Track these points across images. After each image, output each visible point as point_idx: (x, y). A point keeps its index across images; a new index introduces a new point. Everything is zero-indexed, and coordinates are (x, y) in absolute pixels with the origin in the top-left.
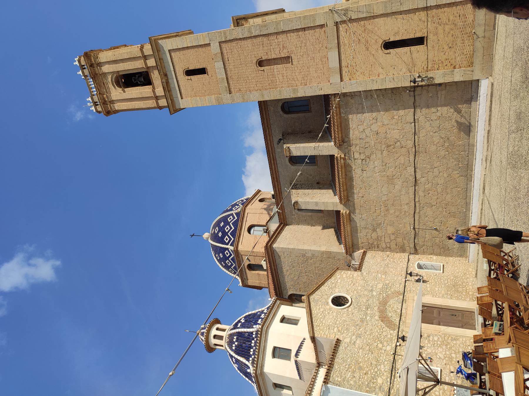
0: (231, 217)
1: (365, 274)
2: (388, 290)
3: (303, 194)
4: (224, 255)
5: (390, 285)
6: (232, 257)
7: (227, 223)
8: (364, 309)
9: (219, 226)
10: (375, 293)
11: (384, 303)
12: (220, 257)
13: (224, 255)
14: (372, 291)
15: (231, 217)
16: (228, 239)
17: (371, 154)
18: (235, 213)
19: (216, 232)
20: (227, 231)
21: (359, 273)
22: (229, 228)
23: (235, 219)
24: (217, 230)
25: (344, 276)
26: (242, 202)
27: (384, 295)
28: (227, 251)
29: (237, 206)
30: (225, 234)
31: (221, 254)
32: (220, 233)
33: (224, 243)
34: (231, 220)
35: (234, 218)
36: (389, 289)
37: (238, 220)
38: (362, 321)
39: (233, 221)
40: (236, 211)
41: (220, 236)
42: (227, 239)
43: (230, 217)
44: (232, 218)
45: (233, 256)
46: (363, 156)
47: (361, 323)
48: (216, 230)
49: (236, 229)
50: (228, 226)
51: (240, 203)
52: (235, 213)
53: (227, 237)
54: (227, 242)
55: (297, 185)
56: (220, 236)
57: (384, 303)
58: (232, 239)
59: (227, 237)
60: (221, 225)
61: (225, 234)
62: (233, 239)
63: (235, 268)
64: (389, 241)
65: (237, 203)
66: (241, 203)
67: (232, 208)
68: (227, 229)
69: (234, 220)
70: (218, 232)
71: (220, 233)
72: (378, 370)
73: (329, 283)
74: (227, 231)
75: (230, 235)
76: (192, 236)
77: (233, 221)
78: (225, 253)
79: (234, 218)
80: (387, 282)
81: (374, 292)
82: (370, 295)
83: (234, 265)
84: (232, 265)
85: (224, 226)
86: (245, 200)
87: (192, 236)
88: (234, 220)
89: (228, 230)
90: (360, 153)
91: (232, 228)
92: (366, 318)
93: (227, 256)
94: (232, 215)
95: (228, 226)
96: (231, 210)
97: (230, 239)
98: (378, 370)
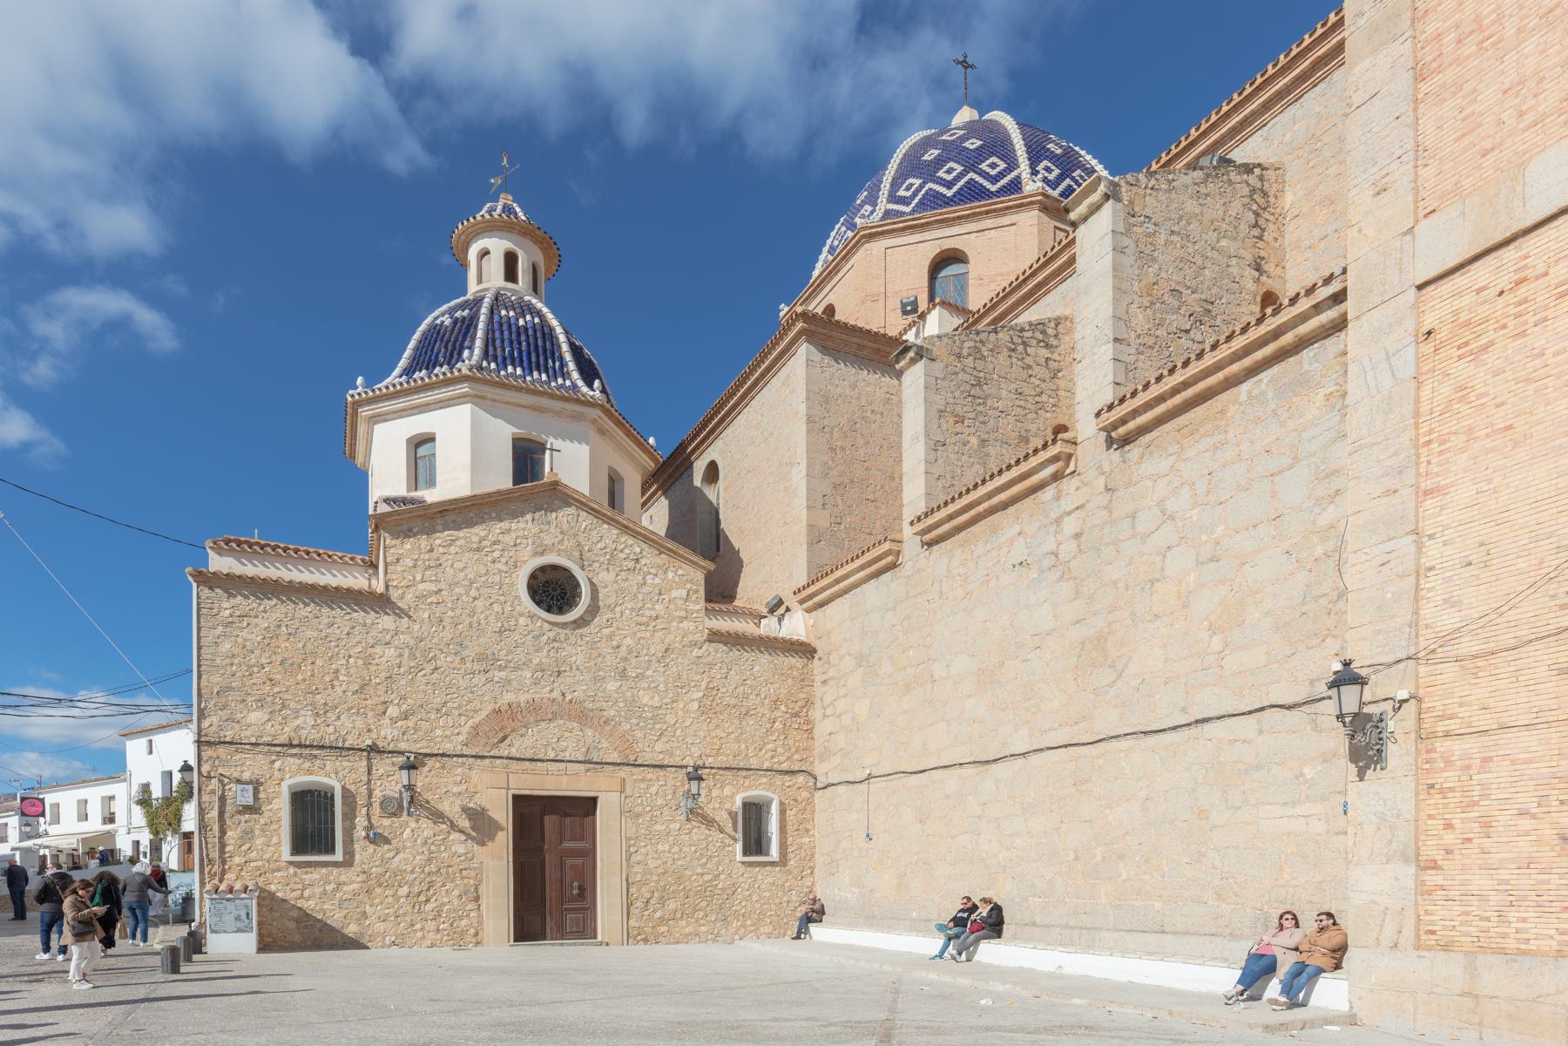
0: (1002, 166)
2: (634, 721)
3: (982, 375)
5: (657, 726)
8: (536, 661)
10: (612, 686)
11: (582, 716)
14: (623, 674)
15: (1002, 166)
27: (612, 712)
34: (988, 170)
35: (1002, 175)
36: (642, 724)
38: (487, 661)
44: (993, 172)
47: (473, 654)
55: (1048, 346)
57: (582, 716)
64: (837, 713)
80: (670, 719)
81: (619, 684)
82: (601, 673)
92: (501, 668)
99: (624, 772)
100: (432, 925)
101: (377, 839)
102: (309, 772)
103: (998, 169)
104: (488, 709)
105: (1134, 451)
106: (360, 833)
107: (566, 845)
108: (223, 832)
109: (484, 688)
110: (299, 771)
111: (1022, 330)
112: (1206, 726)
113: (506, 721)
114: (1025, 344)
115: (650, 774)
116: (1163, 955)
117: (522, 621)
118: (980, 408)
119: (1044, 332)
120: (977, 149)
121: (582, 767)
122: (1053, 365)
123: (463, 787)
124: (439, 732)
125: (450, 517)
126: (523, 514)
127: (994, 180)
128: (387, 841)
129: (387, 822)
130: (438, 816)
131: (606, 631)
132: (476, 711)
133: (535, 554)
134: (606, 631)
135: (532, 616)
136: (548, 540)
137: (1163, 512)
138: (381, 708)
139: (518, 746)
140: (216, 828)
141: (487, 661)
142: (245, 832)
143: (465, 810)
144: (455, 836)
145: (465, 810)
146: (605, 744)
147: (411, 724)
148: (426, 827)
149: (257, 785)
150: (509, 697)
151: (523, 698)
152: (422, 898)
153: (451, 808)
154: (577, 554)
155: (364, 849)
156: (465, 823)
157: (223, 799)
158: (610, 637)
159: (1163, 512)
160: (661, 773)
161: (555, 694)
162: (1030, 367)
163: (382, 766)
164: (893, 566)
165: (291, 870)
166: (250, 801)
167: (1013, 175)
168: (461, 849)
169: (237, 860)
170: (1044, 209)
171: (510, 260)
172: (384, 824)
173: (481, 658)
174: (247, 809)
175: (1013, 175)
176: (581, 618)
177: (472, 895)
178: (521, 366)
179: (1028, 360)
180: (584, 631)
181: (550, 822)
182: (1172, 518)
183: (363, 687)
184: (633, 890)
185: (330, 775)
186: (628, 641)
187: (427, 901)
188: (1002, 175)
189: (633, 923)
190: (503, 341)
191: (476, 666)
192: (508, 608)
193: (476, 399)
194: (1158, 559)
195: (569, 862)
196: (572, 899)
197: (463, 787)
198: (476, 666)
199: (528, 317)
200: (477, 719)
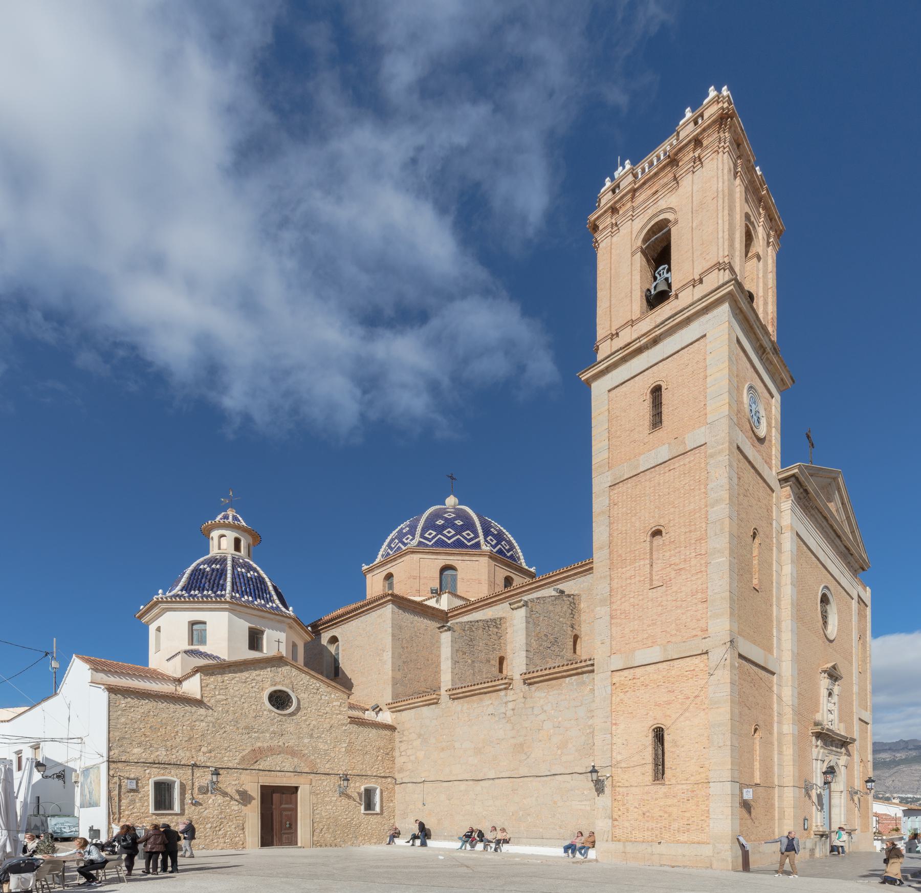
0: (472, 535)
4: (406, 534)
6: (402, 547)
7: (459, 530)
8: (272, 730)
9: (455, 519)
12: (404, 528)
13: (406, 534)
15: (472, 535)
16: (430, 537)
17: (512, 723)
18: (479, 541)
19: (445, 515)
20: (445, 532)
22: (449, 535)
23: (466, 543)
24: (450, 515)
26: (506, 549)
28: (411, 537)
29: (495, 542)
30: (440, 529)
31: (408, 529)
32: (443, 522)
33: (424, 530)
34: (466, 536)
35: (472, 539)
37: (467, 547)
39: (463, 540)
40: (482, 541)
41: (437, 523)
42: (430, 534)
43: (471, 534)
44: (468, 537)
45: (404, 548)
46: (510, 713)
48: (449, 515)
49: (448, 546)
50: (453, 532)
51: (503, 547)
52: (479, 541)
53: (434, 533)
54: (426, 535)
55: (497, 628)
56: (437, 523)
58: (430, 541)
59: (434, 533)
60: (456, 522)
61: (440, 529)
62: (430, 544)
63: (388, 554)
65: (503, 543)
66: (504, 548)
67: (493, 535)
68: (449, 532)
69: (465, 541)
70: (446, 519)
71: (443, 522)
73: (318, 685)
74: (445, 532)
75: (437, 538)
76: (452, 478)
77: (463, 540)
78: (409, 536)
79: (469, 541)
83: (391, 553)
84: (391, 549)
85: (454, 526)
86: (512, 555)
87: (452, 478)
88: (465, 541)
89: (447, 534)
90: (513, 710)
91: (449, 540)
93: (404, 540)
94: (477, 536)
95: (453, 532)
96: (487, 533)
97: (430, 540)
100: (222, 840)
103: (470, 537)
104: (249, 749)
105: (533, 688)
109: (247, 741)
111: (488, 622)
112: (556, 776)
113: (257, 754)
114: (488, 626)
116: (543, 845)
117: (265, 713)
118: (472, 649)
119: (495, 623)
120: (461, 525)
122: (499, 634)
123: (237, 782)
124: (226, 758)
127: (469, 541)
130: (225, 794)
132: (244, 750)
133: (272, 685)
135: (270, 711)
136: (278, 680)
137: (543, 709)
141: (249, 729)
143: (238, 791)
144: (233, 802)
145: (238, 791)
148: (220, 799)
150: (259, 744)
151: (265, 745)
152: (217, 829)
153: (231, 790)
154: (291, 686)
156: (237, 797)
159: (543, 709)
162: (490, 635)
164: (437, 703)
167: (477, 540)
168: (236, 808)
170: (490, 557)
171: (237, 542)
175: (477, 540)
177: (241, 828)
178: (251, 596)
179: (490, 633)
182: (545, 711)
187: (220, 830)
188: (472, 539)
190: (241, 584)
191: (244, 731)
192: (259, 707)
193: (230, 610)
194: (541, 723)
197: (237, 782)
199: (252, 573)
200: (244, 753)
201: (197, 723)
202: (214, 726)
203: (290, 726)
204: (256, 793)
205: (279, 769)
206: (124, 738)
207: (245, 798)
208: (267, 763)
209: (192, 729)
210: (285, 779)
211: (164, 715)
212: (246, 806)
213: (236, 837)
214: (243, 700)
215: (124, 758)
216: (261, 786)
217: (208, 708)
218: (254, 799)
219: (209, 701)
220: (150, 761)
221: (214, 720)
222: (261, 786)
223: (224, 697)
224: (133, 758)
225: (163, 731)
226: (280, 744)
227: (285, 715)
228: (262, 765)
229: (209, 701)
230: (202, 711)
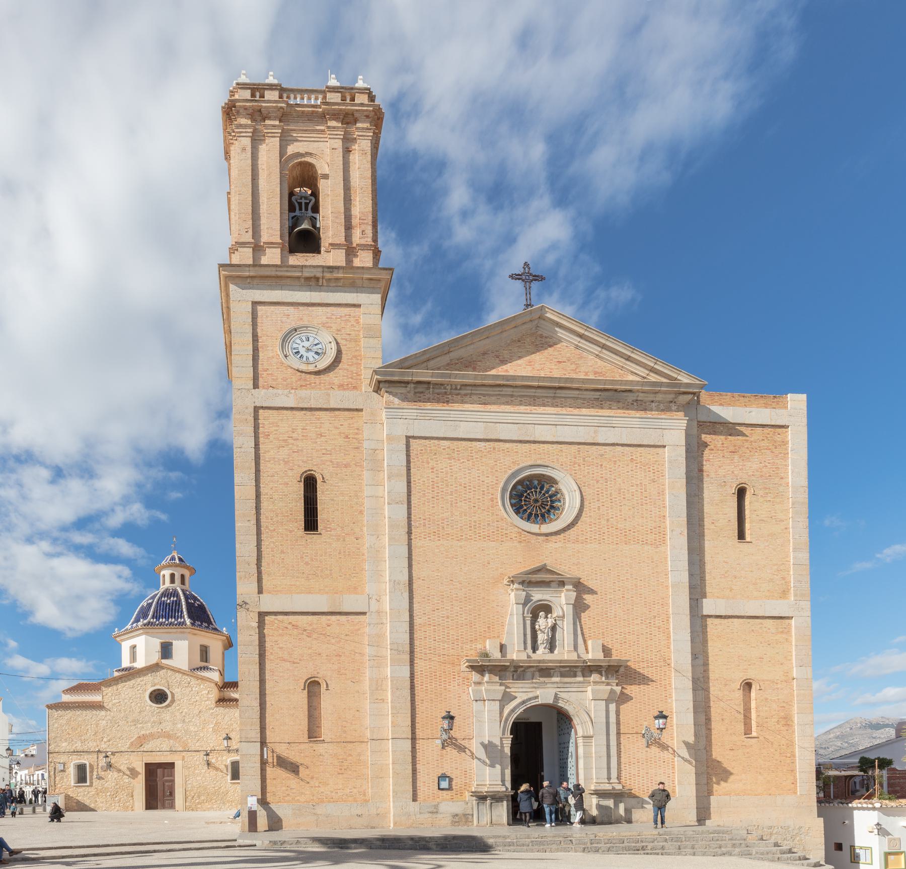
1: (211, 711)
11: (168, 736)
21: (213, 706)
25: (203, 692)
38: (136, 722)
57: (168, 736)
72: (76, 742)
92: (140, 724)
98: (76, 742)
99: (184, 754)
100: (117, 804)
101: (100, 778)
102: (80, 760)
106: (95, 776)
107: (165, 778)
108: (55, 778)
110: (77, 759)
113: (142, 740)
115: (194, 754)
117: (147, 708)
121: (169, 753)
123: (128, 761)
124: (120, 745)
125: (123, 679)
126: (148, 674)
128: (103, 779)
129: (103, 773)
130: (119, 771)
131: (178, 708)
132: (132, 738)
134: (178, 708)
135: (151, 706)
138: (101, 739)
139: (147, 747)
140: (53, 776)
141: (136, 722)
142: (61, 777)
143: (128, 768)
144: (125, 777)
145: (128, 768)
146: (177, 745)
147: (111, 743)
148: (116, 774)
149: (64, 764)
150: (143, 732)
151: (148, 732)
152: (114, 796)
153: (123, 768)
154: (167, 684)
155: (96, 781)
156: (128, 773)
157: (55, 768)
158: (179, 710)
160: (198, 753)
161: (159, 730)
163: (101, 756)
165: (75, 788)
166: (62, 769)
168: (127, 781)
169: (59, 786)
172: (102, 774)
173: (133, 721)
174: (63, 771)
176: (168, 704)
177: (131, 795)
180: (169, 708)
181: (159, 771)
183: (95, 733)
184: (187, 793)
185: (85, 760)
186: (185, 710)
187: (116, 797)
189: (187, 804)
191: (132, 724)
192: (143, 704)
195: (167, 784)
196: (168, 796)
197: (128, 761)
198: (132, 724)
200: (132, 740)
201: (100, 722)
202: (111, 722)
203: (166, 715)
204: (141, 769)
205: (158, 750)
206: (57, 737)
207: (133, 773)
208: (150, 746)
209: (97, 726)
210: (162, 757)
211: (80, 719)
212: (134, 779)
213: (127, 802)
214: (131, 701)
215: (57, 750)
216: (146, 764)
217: (107, 710)
218: (140, 774)
219: (108, 705)
220: (72, 750)
221: (111, 718)
222: (146, 764)
223: (117, 701)
224: (62, 750)
225: (79, 729)
226: (159, 730)
227: (162, 707)
228: (147, 747)
229: (108, 705)
230: (103, 713)
